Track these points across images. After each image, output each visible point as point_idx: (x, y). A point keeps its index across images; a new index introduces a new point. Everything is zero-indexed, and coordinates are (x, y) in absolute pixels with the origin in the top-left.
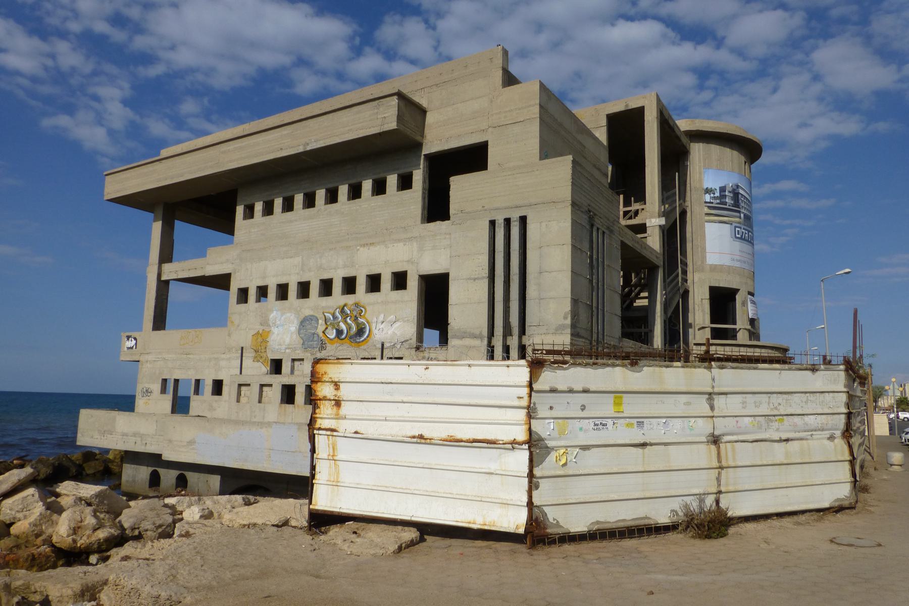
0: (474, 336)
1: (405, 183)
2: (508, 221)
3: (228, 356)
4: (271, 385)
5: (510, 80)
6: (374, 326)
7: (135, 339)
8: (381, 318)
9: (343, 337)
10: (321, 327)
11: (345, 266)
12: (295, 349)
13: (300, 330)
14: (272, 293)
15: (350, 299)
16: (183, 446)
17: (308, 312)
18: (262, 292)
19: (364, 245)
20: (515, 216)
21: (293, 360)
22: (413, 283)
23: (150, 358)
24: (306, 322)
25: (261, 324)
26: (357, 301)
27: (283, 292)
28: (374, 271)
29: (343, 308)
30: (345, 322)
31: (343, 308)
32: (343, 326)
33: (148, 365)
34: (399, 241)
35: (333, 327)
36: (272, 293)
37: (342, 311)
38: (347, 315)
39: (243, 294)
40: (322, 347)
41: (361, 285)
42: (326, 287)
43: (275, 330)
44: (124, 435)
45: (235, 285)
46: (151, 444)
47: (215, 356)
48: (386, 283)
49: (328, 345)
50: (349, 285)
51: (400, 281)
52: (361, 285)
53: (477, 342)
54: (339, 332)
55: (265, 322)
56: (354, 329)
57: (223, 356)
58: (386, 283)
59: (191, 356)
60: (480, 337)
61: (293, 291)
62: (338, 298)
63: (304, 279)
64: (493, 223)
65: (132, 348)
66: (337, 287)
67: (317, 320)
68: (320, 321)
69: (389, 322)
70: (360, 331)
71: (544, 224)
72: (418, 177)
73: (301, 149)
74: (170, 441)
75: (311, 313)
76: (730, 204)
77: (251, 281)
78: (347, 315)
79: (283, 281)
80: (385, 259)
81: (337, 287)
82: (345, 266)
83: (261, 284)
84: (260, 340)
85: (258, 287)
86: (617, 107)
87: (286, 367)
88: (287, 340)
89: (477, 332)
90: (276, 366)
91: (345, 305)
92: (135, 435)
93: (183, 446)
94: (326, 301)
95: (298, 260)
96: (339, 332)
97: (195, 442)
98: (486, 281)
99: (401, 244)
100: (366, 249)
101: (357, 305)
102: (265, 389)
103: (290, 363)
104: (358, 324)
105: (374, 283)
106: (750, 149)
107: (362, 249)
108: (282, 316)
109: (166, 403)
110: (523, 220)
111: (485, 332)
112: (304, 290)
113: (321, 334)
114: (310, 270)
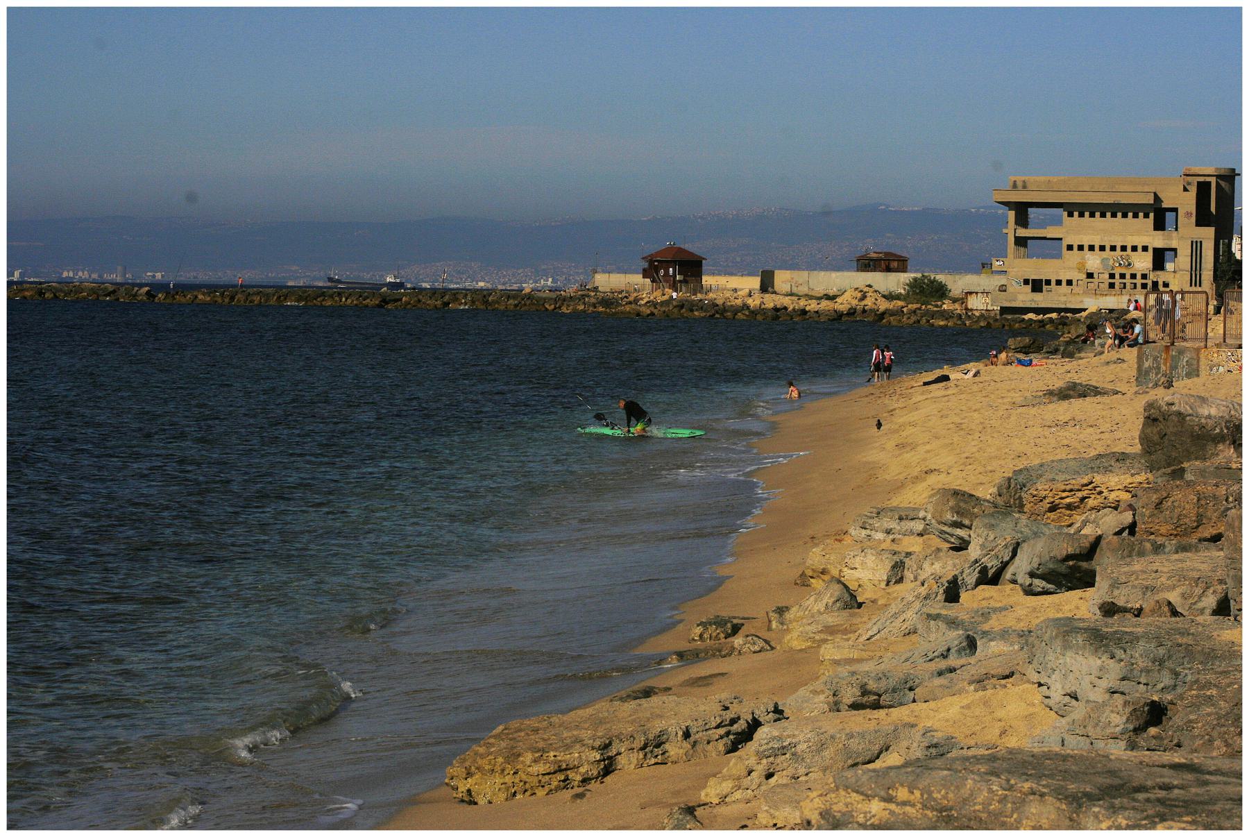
1: (1146, 216)
5: (1185, 190)
10: (1111, 262)
18: (1081, 248)
22: (1150, 250)
24: (1103, 260)
27: (1092, 248)
36: (1086, 248)
39: (1070, 248)
41: (1129, 249)
42: (1113, 248)
45: (1065, 244)
48: (1140, 249)
50: (1124, 248)
51: (1145, 249)
52: (1129, 249)
55: (1083, 258)
58: (1140, 249)
61: (1097, 248)
66: (1118, 249)
72: (1152, 215)
80: (1140, 241)
81: (1118, 249)
86: (1201, 179)
90: (1090, 275)
105: (1134, 249)
109: (1029, 287)
112: (1102, 248)
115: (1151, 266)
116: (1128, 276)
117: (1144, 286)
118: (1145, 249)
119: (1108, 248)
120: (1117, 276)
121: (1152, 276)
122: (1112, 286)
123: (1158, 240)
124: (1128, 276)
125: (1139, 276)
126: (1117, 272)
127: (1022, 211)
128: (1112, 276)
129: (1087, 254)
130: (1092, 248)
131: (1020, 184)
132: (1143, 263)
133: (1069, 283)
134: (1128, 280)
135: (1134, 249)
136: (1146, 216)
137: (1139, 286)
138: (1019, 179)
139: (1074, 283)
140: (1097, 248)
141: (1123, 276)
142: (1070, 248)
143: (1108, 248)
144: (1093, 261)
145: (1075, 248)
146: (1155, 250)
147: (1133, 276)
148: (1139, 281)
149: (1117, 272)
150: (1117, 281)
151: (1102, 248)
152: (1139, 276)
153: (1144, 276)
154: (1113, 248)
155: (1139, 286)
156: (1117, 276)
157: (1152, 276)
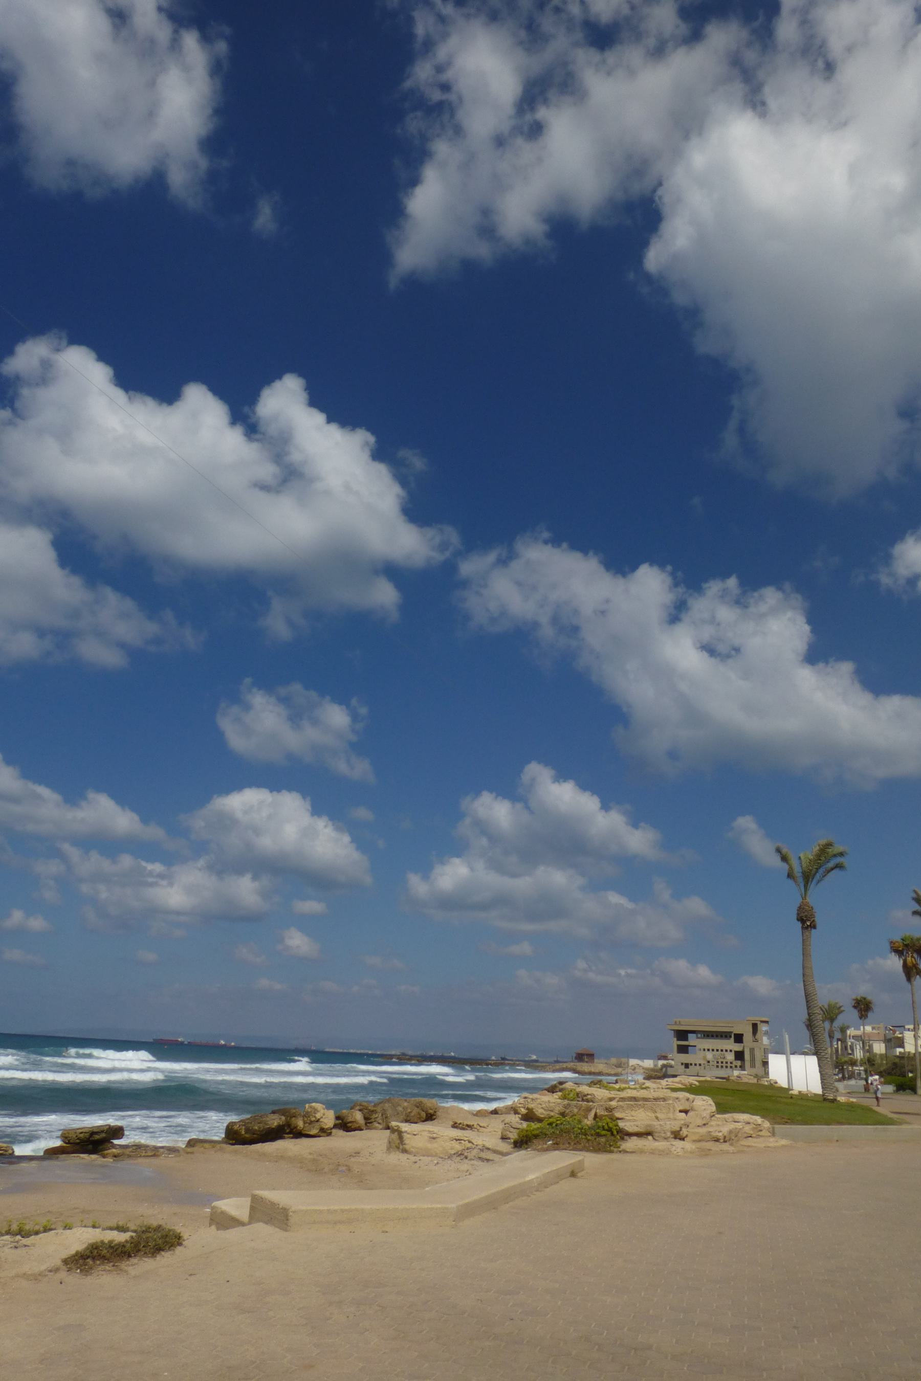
76: (766, 1033)
80: (729, 1047)
106: (767, 1022)
121: (735, 1063)
123: (738, 1047)
126: (720, 1061)
127: (682, 1035)
129: (707, 1053)
132: (730, 1057)
134: (724, 1065)
138: (678, 1020)
144: (709, 1056)
148: (729, 1065)
149: (720, 1061)
150: (720, 1064)
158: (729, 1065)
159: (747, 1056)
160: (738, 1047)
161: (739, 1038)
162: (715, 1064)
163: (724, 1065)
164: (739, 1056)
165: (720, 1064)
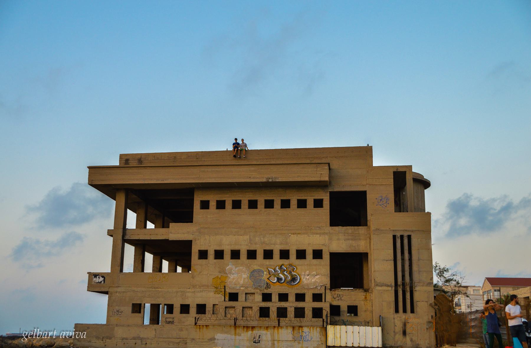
0: (388, 286)
2: (402, 237)
3: (193, 290)
4: (251, 308)
6: (302, 277)
7: (103, 277)
8: (307, 272)
9: (282, 282)
10: (265, 275)
11: (281, 244)
12: (247, 288)
13: (250, 277)
14: (227, 255)
15: (285, 262)
16: (205, 342)
17: (256, 267)
18: (219, 254)
19: (294, 234)
20: (406, 234)
21: (246, 294)
22: (326, 257)
23: (119, 289)
25: (220, 272)
26: (291, 263)
27: (235, 255)
28: (302, 248)
29: (281, 266)
30: (284, 274)
31: (281, 266)
32: (281, 276)
33: (118, 294)
34: (317, 234)
35: (275, 276)
36: (227, 255)
37: (281, 268)
38: (284, 270)
39: (203, 255)
40: (268, 286)
41: (293, 255)
42: (268, 254)
43: (232, 277)
44: (123, 339)
46: (151, 344)
47: (182, 290)
48: (309, 255)
49: (272, 286)
50: (285, 254)
51: (318, 254)
52: (293, 255)
53: (390, 288)
54: (279, 280)
55: (223, 271)
56: (290, 278)
57: (188, 290)
58: (309, 255)
59: (160, 290)
60: (391, 286)
61: (243, 255)
62: (277, 260)
63: (252, 248)
64: (394, 237)
65: (101, 282)
66: (276, 255)
67: (263, 272)
68: (265, 273)
69: (313, 275)
70: (294, 279)
71: (419, 240)
73: (264, 180)
74: (193, 339)
75: (259, 268)
77: (210, 246)
78: (284, 270)
79: (236, 248)
80: (310, 242)
81: (276, 255)
82: (281, 244)
83: (218, 248)
84: (219, 281)
85: (215, 251)
87: (241, 297)
88: (242, 282)
89: (389, 284)
90: (234, 297)
91: (283, 265)
92: (134, 338)
93: (205, 342)
94: (268, 262)
95: (247, 237)
96: (279, 280)
97: (215, 339)
98: (393, 262)
99: (318, 236)
100: (295, 236)
101: (291, 265)
102: (244, 310)
103: (244, 295)
104: (292, 276)
105: (301, 254)
107: (292, 235)
108: (236, 267)
110: (409, 237)
111: (393, 284)
112: (252, 255)
113: (267, 280)
114: (256, 244)
115: (327, 281)
116: (292, 298)
117: (317, 313)
118: (318, 254)
119: (260, 255)
120: (275, 298)
122: (264, 313)
124: (292, 298)
125: (309, 297)
126: (275, 290)
128: (267, 297)
129: (229, 264)
130: (235, 255)
131: (133, 163)
132: (314, 276)
133: (201, 309)
135: (301, 254)
136: (318, 204)
137: (309, 313)
139: (209, 308)
140: (243, 255)
141: (283, 297)
142: (203, 255)
143: (260, 255)
144: (238, 275)
145: (211, 255)
146: (333, 256)
147: (300, 297)
148: (309, 305)
149: (275, 290)
150: (274, 305)
151: (252, 255)
152: (309, 297)
153: (317, 297)
154: (268, 254)
155: (309, 313)
156: (275, 298)
157: (331, 298)
158: (309, 305)
159: (380, 269)
160: (342, 240)
161: (349, 209)
162: (257, 300)
163: (291, 305)
164: (348, 270)
165: (274, 305)
